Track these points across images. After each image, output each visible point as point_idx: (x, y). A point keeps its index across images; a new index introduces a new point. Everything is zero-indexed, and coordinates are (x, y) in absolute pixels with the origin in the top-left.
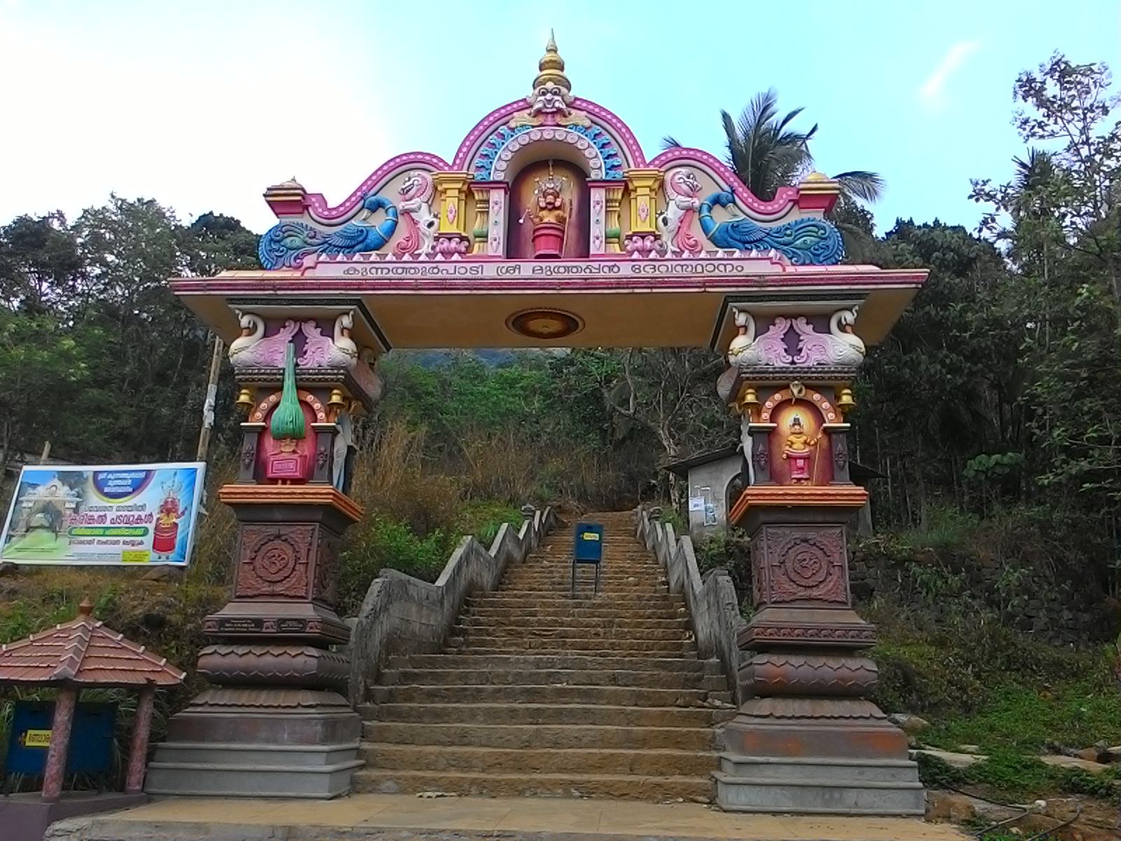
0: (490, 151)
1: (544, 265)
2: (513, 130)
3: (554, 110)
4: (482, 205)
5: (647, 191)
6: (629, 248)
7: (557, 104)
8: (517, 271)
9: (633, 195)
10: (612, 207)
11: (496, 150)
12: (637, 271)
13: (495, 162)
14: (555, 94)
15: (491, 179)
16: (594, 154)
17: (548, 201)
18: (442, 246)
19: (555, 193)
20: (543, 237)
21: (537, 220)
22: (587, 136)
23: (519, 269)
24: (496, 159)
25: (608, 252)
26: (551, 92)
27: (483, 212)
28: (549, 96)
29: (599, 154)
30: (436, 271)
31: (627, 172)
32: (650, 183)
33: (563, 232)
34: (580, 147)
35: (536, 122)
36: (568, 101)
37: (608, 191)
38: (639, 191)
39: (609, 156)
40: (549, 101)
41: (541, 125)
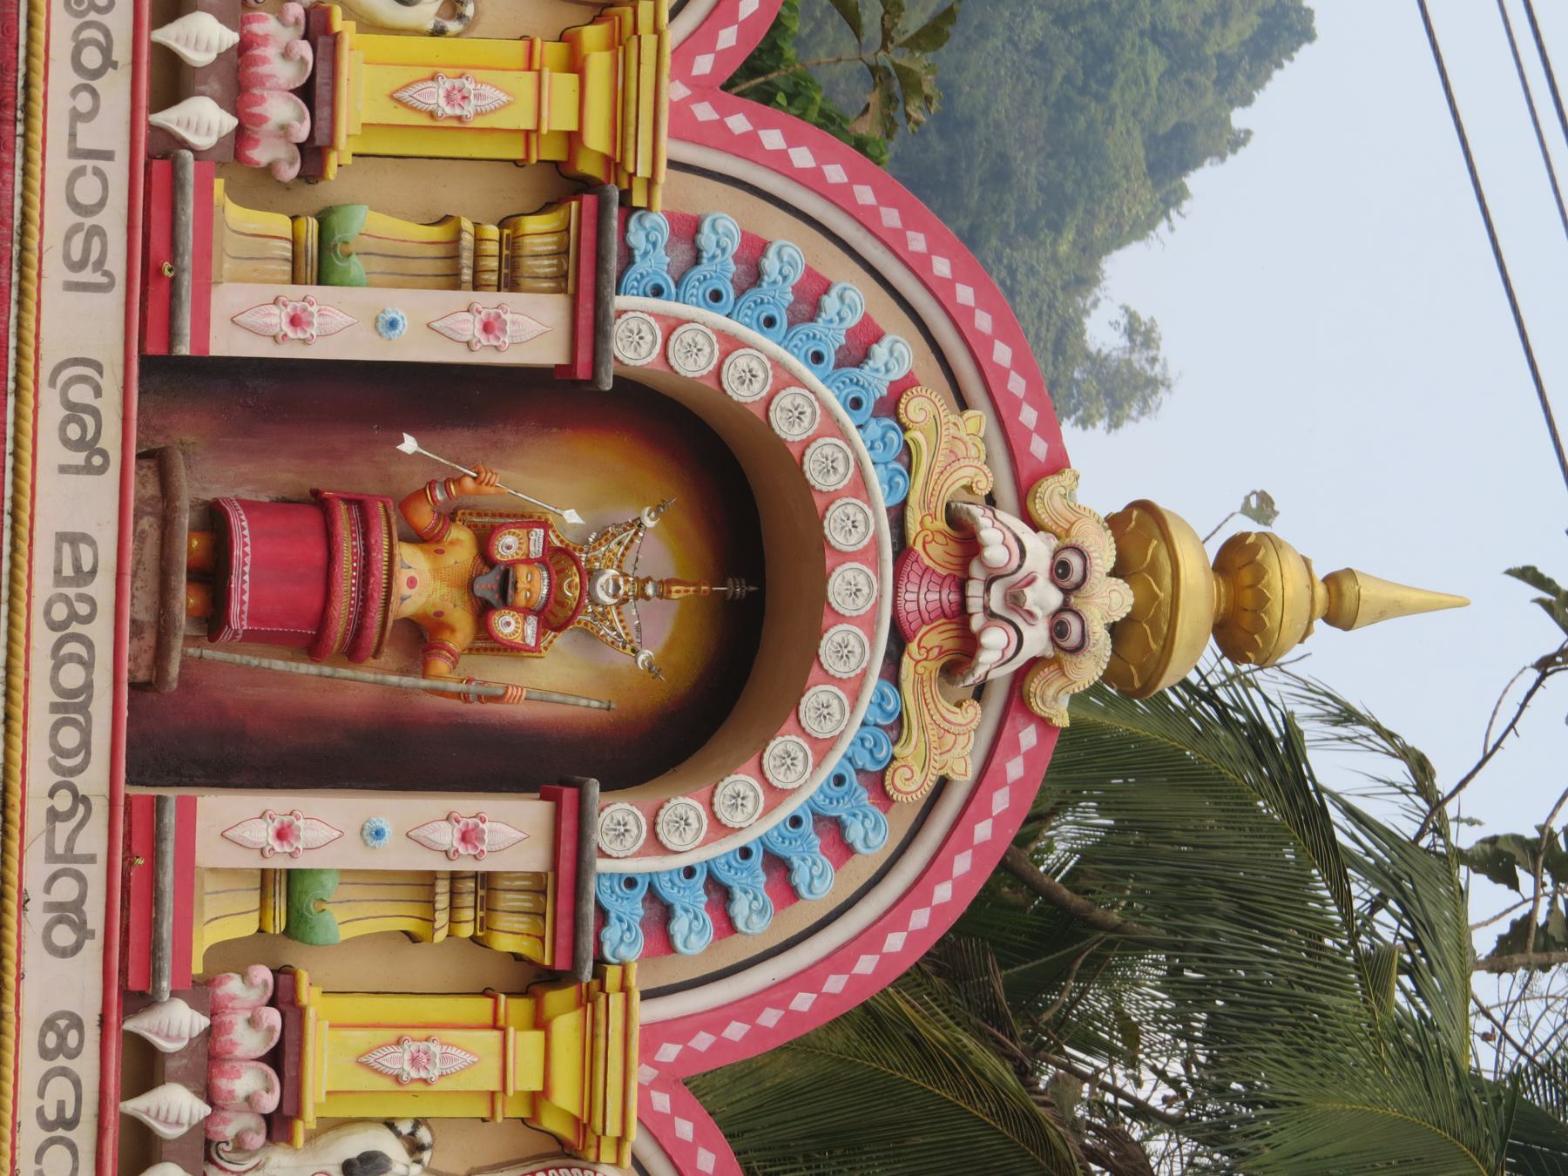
0: (778, 292)
1: (102, 589)
2: (890, 406)
3: (976, 623)
4: (492, 248)
5: (526, 1078)
6: (233, 986)
7: (995, 640)
8: (79, 458)
9: (518, 1009)
10: (453, 907)
11: (782, 321)
12: (51, 1040)
13: (718, 319)
14: (1058, 630)
15: (619, 302)
16: (669, 838)
17: (523, 572)
18: (271, 52)
19: (563, 614)
20: (319, 554)
21: (424, 517)
22: (839, 780)
23: (88, 469)
24: (733, 326)
25: (206, 885)
26: (1065, 607)
27: (454, 256)
28: (1042, 597)
29: (733, 843)
30: (92, 58)
31: (624, 989)
32: (566, 1097)
33: (353, 652)
34: (776, 747)
35: (924, 525)
36: (1035, 685)
37: (537, 886)
38: (527, 1043)
39: (720, 893)
40: (1015, 600)
41: (902, 550)
